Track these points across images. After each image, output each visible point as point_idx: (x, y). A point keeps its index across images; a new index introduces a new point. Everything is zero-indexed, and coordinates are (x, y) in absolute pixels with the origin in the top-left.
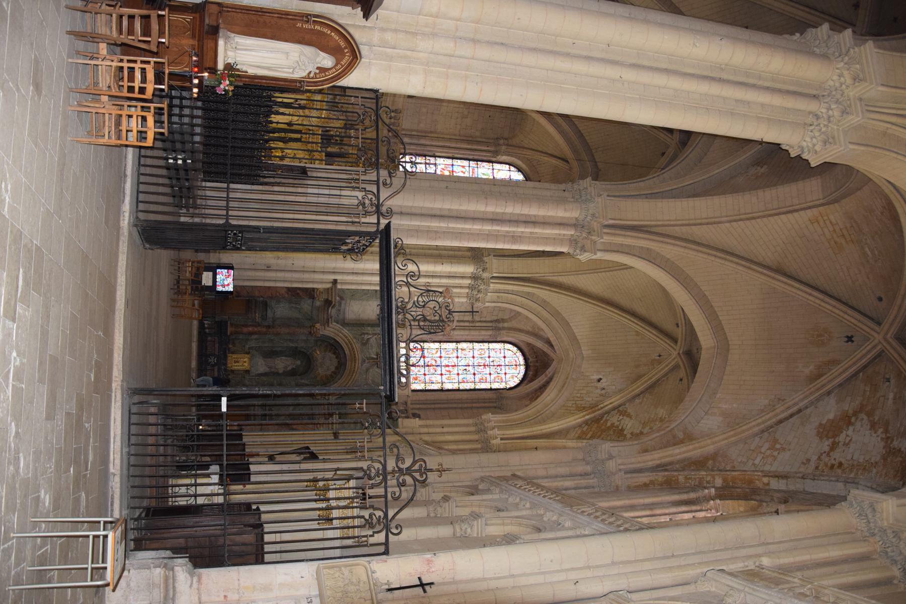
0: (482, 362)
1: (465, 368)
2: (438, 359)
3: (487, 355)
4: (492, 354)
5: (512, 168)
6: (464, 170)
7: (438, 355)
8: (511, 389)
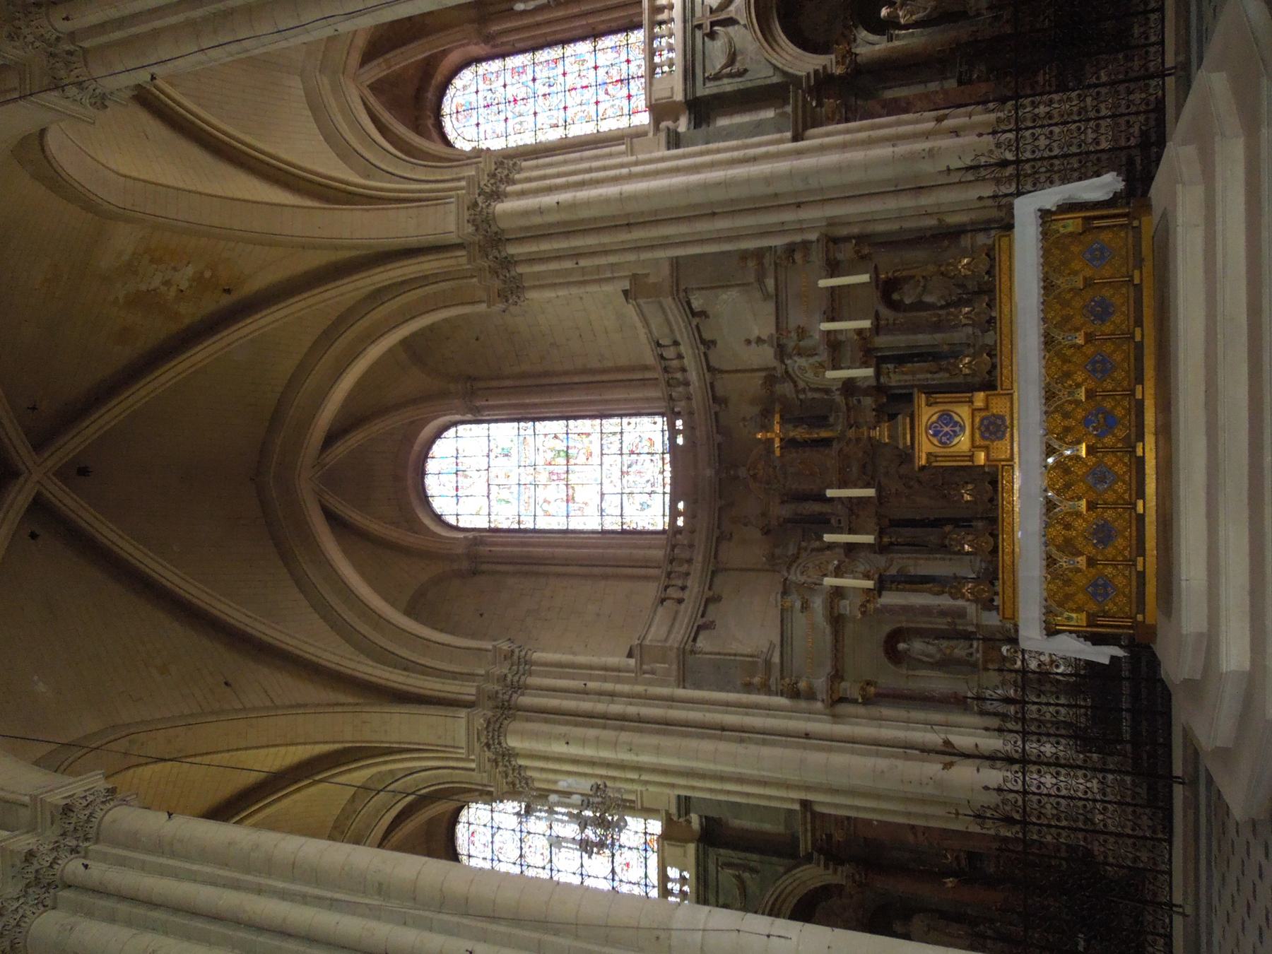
0: (520, 107)
1: (553, 89)
2: (602, 97)
3: (510, 122)
4: (500, 127)
5: (452, 521)
6: (546, 506)
7: (601, 107)
8: (466, 64)
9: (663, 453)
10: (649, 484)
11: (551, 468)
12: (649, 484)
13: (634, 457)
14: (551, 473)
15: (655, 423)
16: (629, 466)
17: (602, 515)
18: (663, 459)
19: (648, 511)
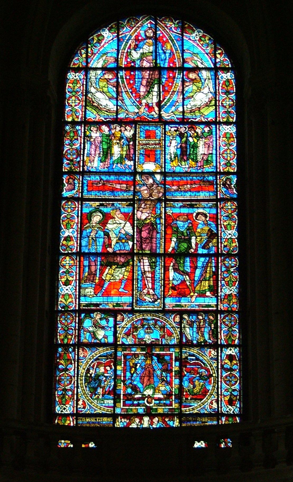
5: (79, 61)
6: (97, 218)
9: (181, 416)
10: (129, 390)
11: (161, 228)
12: (129, 390)
13: (176, 366)
14: (152, 227)
15: (231, 402)
16: (160, 358)
17: (80, 311)
18: (171, 415)
19: (84, 390)
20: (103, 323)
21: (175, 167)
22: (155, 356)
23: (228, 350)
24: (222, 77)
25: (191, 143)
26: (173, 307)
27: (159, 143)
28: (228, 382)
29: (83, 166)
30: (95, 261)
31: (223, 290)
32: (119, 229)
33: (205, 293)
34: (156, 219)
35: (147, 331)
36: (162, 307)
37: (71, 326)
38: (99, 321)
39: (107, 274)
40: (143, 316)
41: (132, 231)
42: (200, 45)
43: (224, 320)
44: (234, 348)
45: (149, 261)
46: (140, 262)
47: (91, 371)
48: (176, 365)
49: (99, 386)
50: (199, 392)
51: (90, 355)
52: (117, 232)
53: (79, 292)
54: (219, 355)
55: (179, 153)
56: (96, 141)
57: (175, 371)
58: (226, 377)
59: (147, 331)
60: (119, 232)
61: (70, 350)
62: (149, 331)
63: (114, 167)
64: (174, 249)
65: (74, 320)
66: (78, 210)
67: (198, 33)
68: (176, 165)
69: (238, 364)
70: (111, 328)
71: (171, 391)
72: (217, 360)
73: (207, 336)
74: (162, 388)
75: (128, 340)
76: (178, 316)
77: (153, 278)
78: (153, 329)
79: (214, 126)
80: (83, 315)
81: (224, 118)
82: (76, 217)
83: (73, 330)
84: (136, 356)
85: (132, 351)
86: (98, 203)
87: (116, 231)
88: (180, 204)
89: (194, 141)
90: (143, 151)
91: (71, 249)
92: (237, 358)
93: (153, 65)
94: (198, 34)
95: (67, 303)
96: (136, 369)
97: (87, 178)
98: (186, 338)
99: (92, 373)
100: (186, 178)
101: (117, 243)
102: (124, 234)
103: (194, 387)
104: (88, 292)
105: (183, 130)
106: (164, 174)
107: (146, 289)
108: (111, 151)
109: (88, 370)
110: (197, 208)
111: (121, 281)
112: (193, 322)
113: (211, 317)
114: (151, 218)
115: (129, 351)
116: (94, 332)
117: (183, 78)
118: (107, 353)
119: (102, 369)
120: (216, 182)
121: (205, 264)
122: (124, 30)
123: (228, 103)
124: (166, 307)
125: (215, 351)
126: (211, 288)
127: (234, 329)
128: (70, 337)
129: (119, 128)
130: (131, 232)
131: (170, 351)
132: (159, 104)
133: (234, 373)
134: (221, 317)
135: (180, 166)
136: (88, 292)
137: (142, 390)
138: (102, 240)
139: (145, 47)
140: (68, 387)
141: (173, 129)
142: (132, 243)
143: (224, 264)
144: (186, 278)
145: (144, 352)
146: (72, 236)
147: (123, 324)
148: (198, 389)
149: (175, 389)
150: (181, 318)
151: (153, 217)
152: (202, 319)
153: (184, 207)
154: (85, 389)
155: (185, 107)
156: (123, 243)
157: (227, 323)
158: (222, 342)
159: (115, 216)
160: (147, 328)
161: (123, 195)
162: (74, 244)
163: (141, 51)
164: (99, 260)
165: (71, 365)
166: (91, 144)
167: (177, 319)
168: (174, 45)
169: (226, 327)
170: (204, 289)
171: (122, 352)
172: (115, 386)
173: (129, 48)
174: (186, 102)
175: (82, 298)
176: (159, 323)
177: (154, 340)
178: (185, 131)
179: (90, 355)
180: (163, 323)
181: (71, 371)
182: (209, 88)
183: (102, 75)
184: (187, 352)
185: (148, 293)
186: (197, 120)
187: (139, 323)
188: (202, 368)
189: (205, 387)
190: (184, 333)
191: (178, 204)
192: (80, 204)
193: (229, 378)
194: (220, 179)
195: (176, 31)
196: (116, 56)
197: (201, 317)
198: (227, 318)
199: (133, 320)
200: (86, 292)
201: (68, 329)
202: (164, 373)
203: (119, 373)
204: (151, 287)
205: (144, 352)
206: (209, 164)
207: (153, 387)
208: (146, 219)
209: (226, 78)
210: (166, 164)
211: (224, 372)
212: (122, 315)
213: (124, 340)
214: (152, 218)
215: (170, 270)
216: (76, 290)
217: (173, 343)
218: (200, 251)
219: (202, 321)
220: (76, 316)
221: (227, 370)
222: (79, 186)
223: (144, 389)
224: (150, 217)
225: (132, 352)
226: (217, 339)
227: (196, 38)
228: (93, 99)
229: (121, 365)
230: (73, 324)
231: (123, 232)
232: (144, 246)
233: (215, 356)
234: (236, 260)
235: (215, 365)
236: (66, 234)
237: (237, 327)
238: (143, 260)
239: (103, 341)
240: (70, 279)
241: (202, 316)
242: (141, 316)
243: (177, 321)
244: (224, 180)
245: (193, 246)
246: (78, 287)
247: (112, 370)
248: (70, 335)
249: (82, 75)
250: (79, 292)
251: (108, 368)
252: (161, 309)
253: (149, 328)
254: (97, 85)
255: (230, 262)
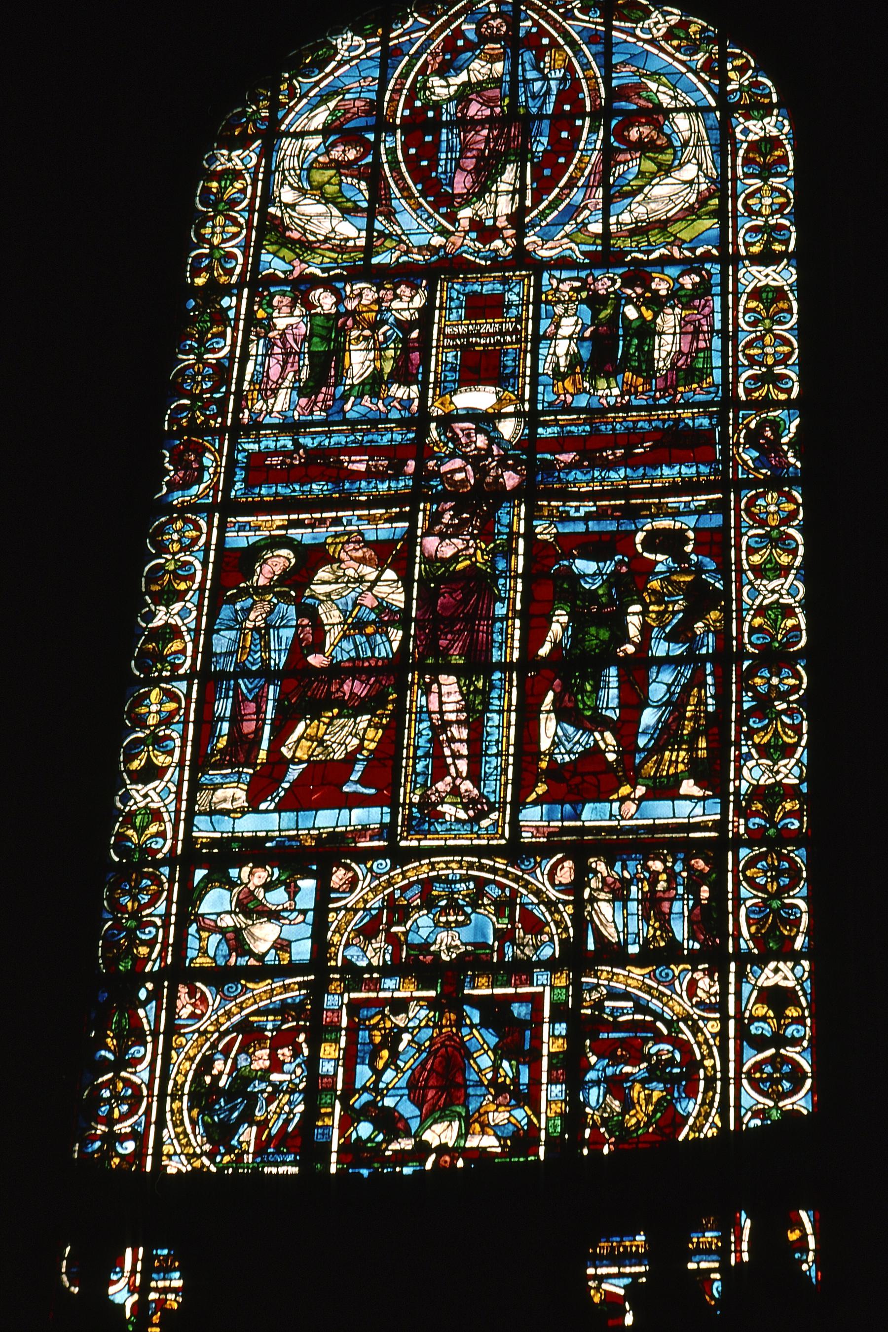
12: (365, 1129)
20: (277, 898)
21: (572, 395)
22: (473, 1006)
23: (768, 971)
24: (746, 131)
25: (631, 321)
26: (550, 835)
27: (515, 328)
28: (765, 1087)
29: (238, 409)
30: (260, 699)
31: (745, 772)
32: (353, 594)
33: (679, 785)
34: (495, 556)
35: (443, 919)
36: (507, 835)
37: (151, 915)
38: (260, 893)
39: (298, 741)
40: (433, 869)
41: (402, 597)
42: (670, 49)
43: (748, 873)
44: (790, 964)
45: (460, 687)
46: (427, 692)
47: (218, 1066)
48: (557, 1033)
49: (247, 1117)
50: (647, 1125)
51: (218, 1009)
52: (347, 604)
53: (192, 801)
54: (732, 989)
55: (585, 354)
56: (290, 338)
57: (551, 1055)
58: (757, 1066)
59: (443, 919)
60: (355, 604)
61: (143, 995)
62: (452, 918)
63: (348, 407)
64: (557, 646)
65: (165, 894)
66: (208, 543)
67: (664, 17)
68: (571, 390)
69: (808, 1021)
70: (304, 912)
71: (534, 1130)
72: (722, 1007)
73: (680, 929)
74: (499, 1117)
75: (370, 953)
76: (568, 864)
77: (476, 742)
78: (468, 910)
79: (716, 269)
80: (200, 874)
81: (753, 244)
82: (198, 566)
83: (157, 928)
84: (400, 1006)
85: (381, 990)
86: (280, 519)
87: (343, 600)
88: (589, 507)
89: (641, 316)
90: (456, 356)
91: (173, 665)
92: (803, 999)
93: (502, 111)
94: (662, 20)
95: (143, 838)
96: (395, 1055)
97: (246, 446)
98: (598, 935)
99: (221, 1073)
100: (609, 427)
101: (345, 636)
102: (372, 609)
103: (628, 1104)
104: (225, 800)
105: (602, 287)
106: (532, 419)
107: (448, 779)
108: (340, 361)
109: (207, 1064)
110: (653, 517)
111: (351, 759)
112: (626, 884)
113: (700, 864)
114: (475, 554)
115: (369, 991)
116: (238, 931)
117: (606, 140)
118: (282, 1001)
119: (261, 1059)
120: (724, 435)
121: (678, 690)
122: (405, 27)
123: (767, 201)
124: (524, 834)
125: (712, 979)
126: (701, 768)
127: (787, 901)
128: (143, 950)
129: (371, 294)
130: (398, 599)
131: (531, 985)
132: (517, 219)
133: (790, 1052)
134: (736, 861)
135: (589, 393)
136: (225, 800)
137: (414, 1125)
138: (287, 634)
139: (475, 65)
140: (124, 1128)
141: (565, 287)
142: (400, 633)
143: (753, 688)
144: (603, 739)
145: (432, 993)
146: (180, 623)
147: (351, 900)
148: (641, 1116)
149: (548, 1119)
150: (583, 872)
151: (482, 551)
152: (664, 871)
153: (600, 515)
154: (189, 1130)
155: (613, 220)
156: (368, 636)
157: (761, 881)
158: (743, 945)
159: (343, 555)
160: (444, 911)
161: (376, 487)
162: (185, 647)
163: (463, 77)
164: (271, 696)
165: (142, 1049)
166: (270, 345)
167: (566, 874)
168: (577, 51)
169: (756, 897)
170: (672, 770)
171: (341, 995)
172: (312, 1115)
173: (422, 71)
174: (615, 208)
175: (201, 821)
176: (494, 891)
177: (469, 948)
178: (612, 289)
179: (218, 1009)
180: (507, 890)
181: (139, 1068)
182: (700, 165)
183: (322, 149)
184: (598, 985)
185: (455, 791)
186: (655, 255)
187: (416, 889)
188: (659, 1038)
189: (671, 1106)
190: (592, 921)
191: (577, 509)
192: (216, 523)
193: (768, 1069)
194: (736, 424)
195: (587, 18)
196: (373, 96)
197: (657, 866)
198: (761, 864)
199: (393, 885)
200: (214, 800)
201: (142, 925)
202: (505, 1064)
203: (327, 1068)
204: (464, 775)
205: (432, 993)
206: (696, 379)
207: (460, 1116)
208: (455, 558)
209: (762, 134)
210: (541, 389)
211: (748, 1051)
212: (348, 868)
213: (353, 953)
214: (479, 552)
215: (543, 717)
216: (178, 793)
217: (546, 952)
218: (660, 649)
219: (664, 877)
220: (171, 881)
221: (760, 1043)
222: (215, 473)
223: (422, 1123)
224: (472, 551)
225: (382, 995)
226: (725, 936)
227: (654, 31)
228: (287, 221)
229: (337, 1041)
230: (161, 908)
231: (369, 601)
232: (443, 643)
233: (715, 995)
234: (798, 672)
235: (714, 1027)
236: (157, 622)
237: (804, 893)
238: (440, 685)
239: (270, 959)
240: (161, 760)
241: (664, 862)
242: (425, 869)
243: (564, 881)
244: (753, 425)
245: (633, 632)
246: (186, 785)
247: (298, 1061)
248: (144, 943)
249: (252, 154)
250: (192, 801)
251: (285, 1053)
252: (503, 842)
253: (454, 906)
254: (304, 178)
255: (775, 681)
